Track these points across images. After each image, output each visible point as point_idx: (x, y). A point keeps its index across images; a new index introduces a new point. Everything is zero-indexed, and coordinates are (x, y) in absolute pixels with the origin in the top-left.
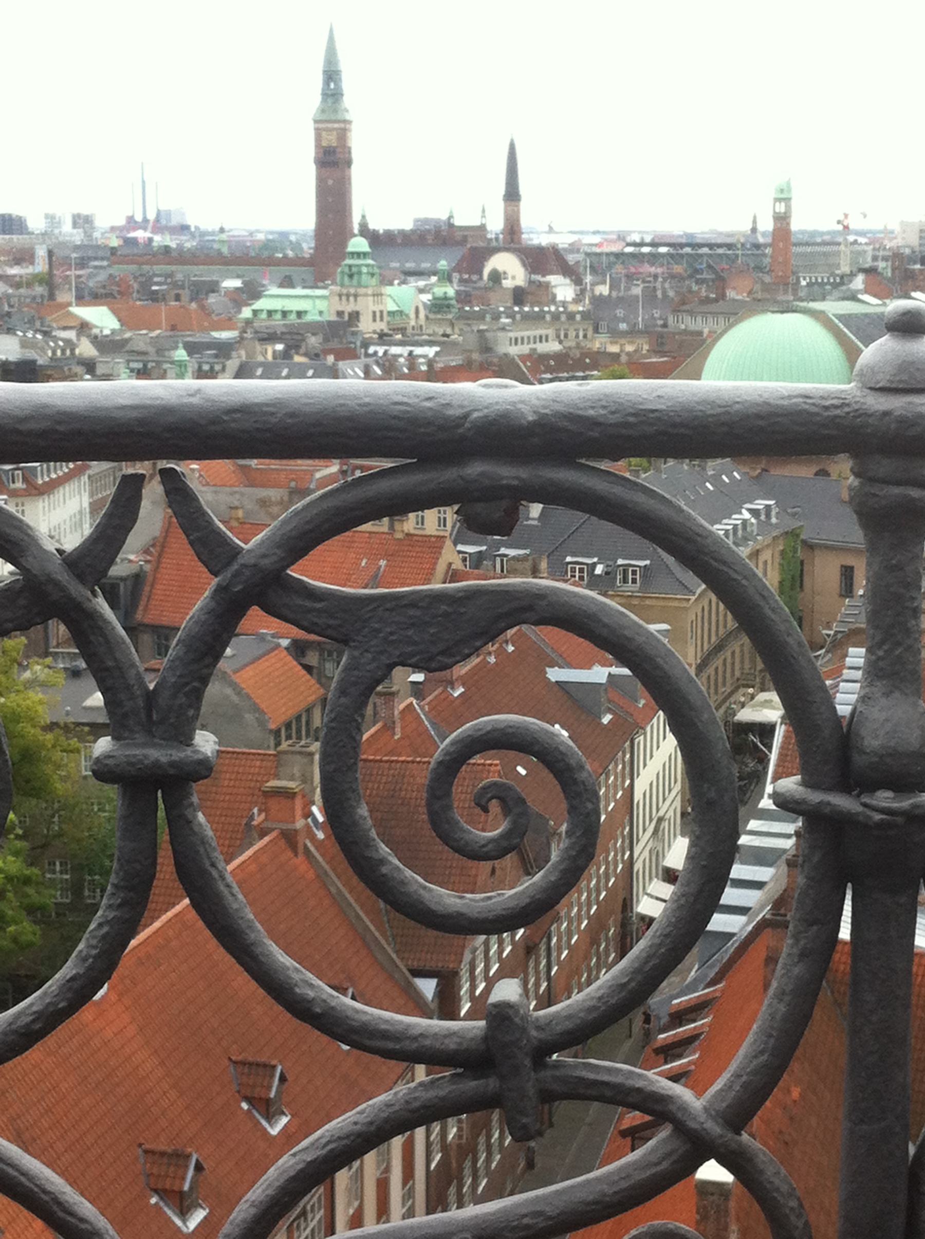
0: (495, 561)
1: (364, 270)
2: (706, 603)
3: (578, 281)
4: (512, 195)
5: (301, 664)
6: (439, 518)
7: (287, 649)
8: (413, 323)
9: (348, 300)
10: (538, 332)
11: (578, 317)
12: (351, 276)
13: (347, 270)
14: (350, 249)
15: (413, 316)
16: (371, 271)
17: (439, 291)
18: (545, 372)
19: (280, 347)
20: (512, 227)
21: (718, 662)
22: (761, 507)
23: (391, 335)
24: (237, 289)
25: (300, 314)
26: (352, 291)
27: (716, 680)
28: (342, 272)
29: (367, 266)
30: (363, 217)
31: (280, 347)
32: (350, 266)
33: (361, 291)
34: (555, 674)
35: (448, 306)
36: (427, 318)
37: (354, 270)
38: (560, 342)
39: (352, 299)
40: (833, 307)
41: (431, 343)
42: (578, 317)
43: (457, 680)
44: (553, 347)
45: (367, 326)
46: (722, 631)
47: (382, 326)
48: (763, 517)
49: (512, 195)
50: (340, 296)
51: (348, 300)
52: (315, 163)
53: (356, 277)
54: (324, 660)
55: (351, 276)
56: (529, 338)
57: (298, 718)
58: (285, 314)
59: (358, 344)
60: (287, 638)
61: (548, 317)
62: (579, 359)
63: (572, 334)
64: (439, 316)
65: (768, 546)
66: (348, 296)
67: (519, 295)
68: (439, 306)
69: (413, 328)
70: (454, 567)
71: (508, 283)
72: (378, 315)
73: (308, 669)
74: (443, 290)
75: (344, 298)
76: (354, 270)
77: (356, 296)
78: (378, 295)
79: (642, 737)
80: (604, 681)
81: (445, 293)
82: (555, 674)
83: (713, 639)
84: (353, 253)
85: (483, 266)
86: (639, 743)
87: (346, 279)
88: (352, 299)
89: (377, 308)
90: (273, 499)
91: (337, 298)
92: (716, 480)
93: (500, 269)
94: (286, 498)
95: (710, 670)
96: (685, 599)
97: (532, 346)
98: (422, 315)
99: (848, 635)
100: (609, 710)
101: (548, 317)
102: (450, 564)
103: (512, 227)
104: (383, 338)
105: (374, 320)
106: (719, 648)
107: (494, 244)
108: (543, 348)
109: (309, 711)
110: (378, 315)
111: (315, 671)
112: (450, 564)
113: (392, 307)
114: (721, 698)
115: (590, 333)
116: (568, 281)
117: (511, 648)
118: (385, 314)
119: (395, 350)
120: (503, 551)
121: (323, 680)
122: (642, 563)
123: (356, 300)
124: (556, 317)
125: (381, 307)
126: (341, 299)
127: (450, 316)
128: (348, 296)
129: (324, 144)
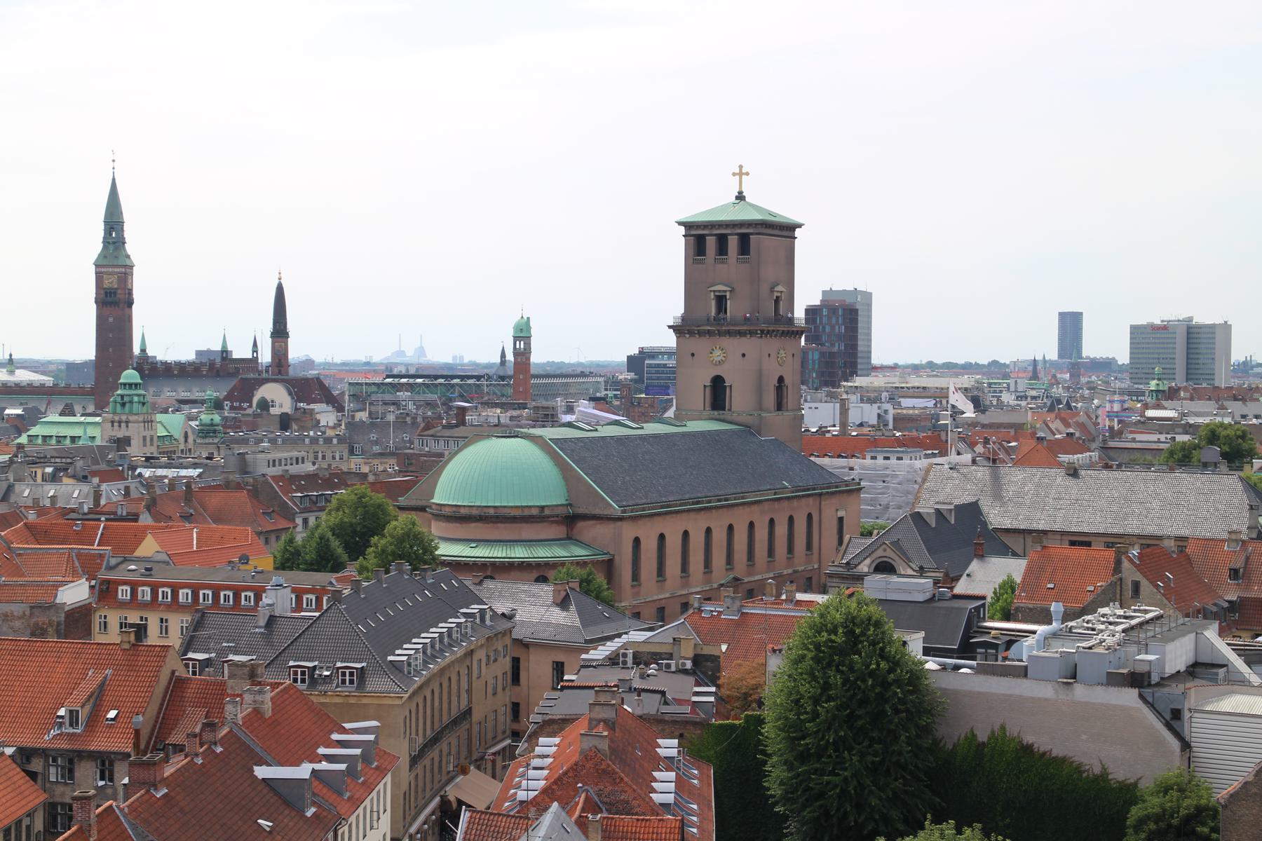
0: (223, 666)
1: (136, 399)
2: (421, 701)
3: (340, 408)
4: (280, 332)
5: (24, 770)
6: (182, 627)
7: (12, 757)
8: (182, 447)
9: (120, 426)
10: (295, 454)
11: (335, 441)
12: (123, 405)
13: (119, 399)
14: (121, 381)
15: (182, 440)
16: (142, 400)
17: (205, 418)
18: (296, 491)
19: (49, 470)
20: (280, 360)
21: (434, 753)
22: (476, 611)
23: (158, 458)
24: (18, 415)
25: (73, 439)
26: (124, 418)
27: (432, 769)
28: (115, 402)
29: (139, 395)
30: (143, 350)
31: (49, 470)
32: (122, 396)
33: (131, 418)
34: (261, 772)
35: (215, 432)
36: (195, 441)
37: (126, 399)
38: (314, 464)
39: (123, 425)
40: (549, 433)
41: (195, 466)
42: (335, 441)
43: (160, 782)
44: (309, 468)
45: (136, 451)
46: (436, 725)
47: (151, 450)
48: (478, 621)
49: (280, 332)
50: (113, 422)
51: (120, 426)
52: (96, 302)
53: (127, 405)
54: (49, 765)
55: (123, 405)
56: (280, 460)
57: (18, 823)
58: (60, 439)
59: (126, 466)
60: (12, 746)
61: (307, 441)
62: (328, 479)
63: (329, 455)
64: (207, 441)
65: (482, 646)
66: (120, 422)
67: (285, 422)
68: (207, 431)
69: (182, 451)
70: (177, 674)
71: (275, 411)
72: (148, 439)
73: (33, 776)
74: (210, 417)
75: (116, 424)
76: (126, 399)
77: (127, 422)
78: (149, 422)
79: (347, 827)
80: (307, 777)
81: (212, 420)
82: (261, 772)
83: (429, 732)
84: (125, 384)
85: (253, 396)
86: (343, 833)
87: (119, 407)
88: (123, 425)
89: (148, 434)
90: (15, 614)
91: (110, 424)
92: (434, 587)
93: (269, 398)
94: (28, 613)
95: (426, 761)
96: (398, 697)
97: (287, 468)
98: (191, 440)
99: (542, 726)
100: (314, 804)
101: (307, 441)
102: (173, 672)
103: (280, 360)
104: (150, 461)
105: (145, 445)
106: (435, 740)
107: (264, 375)
108: (294, 469)
109: (30, 815)
110: (148, 439)
111: (40, 777)
112: (173, 672)
113: (161, 432)
114: (437, 786)
115: (346, 454)
116: (330, 408)
117: (219, 749)
118: (155, 439)
119: (160, 472)
120: (231, 657)
121: (48, 785)
122: (359, 665)
123: (127, 426)
124: (314, 441)
125: (152, 433)
126: (113, 426)
127: (216, 441)
128: (120, 422)
129: (106, 284)
